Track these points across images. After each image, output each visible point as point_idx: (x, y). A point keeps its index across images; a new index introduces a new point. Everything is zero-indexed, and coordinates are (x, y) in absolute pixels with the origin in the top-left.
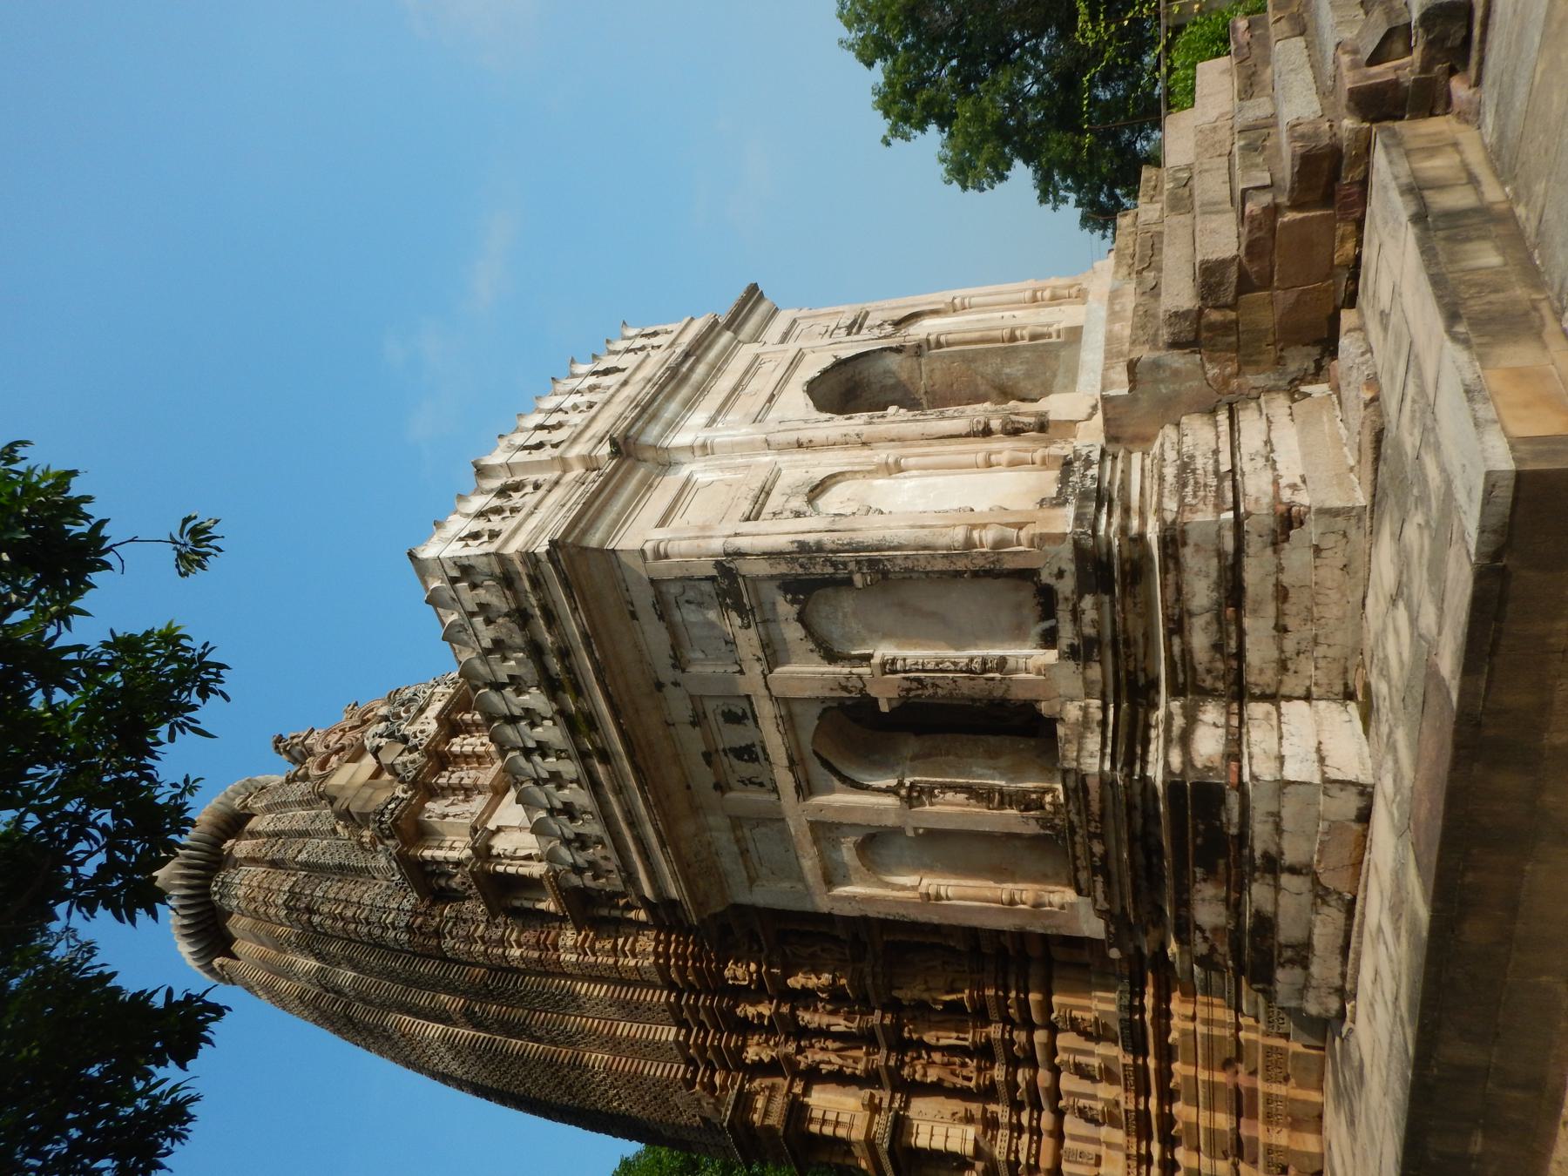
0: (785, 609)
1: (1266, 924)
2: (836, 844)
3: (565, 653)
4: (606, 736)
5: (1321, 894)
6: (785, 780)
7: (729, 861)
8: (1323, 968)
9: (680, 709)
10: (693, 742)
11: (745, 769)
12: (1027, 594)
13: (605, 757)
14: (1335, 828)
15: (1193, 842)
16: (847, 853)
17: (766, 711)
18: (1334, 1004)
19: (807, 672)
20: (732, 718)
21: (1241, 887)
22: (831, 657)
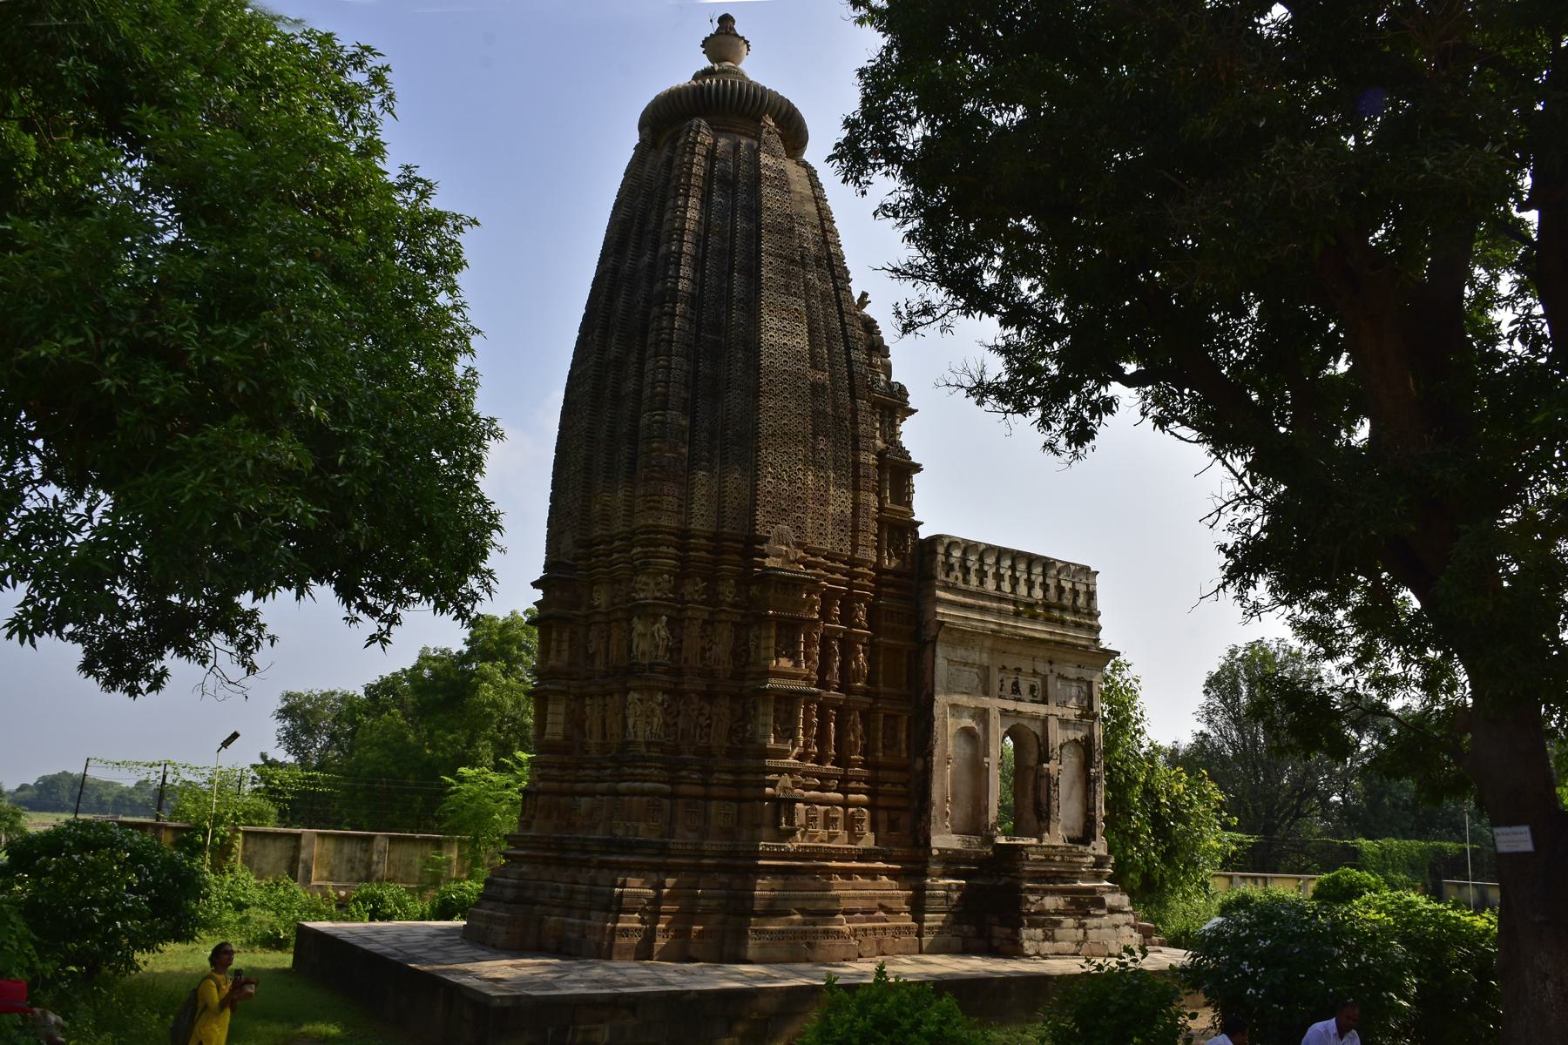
0: (1080, 735)
1: (1058, 924)
2: (973, 717)
3: (1063, 623)
4: (1024, 621)
5: (1079, 943)
6: (1010, 705)
7: (960, 653)
8: (1047, 947)
9: (1042, 668)
10: (1026, 666)
11: (1008, 684)
12: (1078, 833)
13: (1017, 614)
14: (1106, 947)
15: (1082, 897)
16: (967, 722)
17: (1042, 710)
18: (1030, 952)
19: (1057, 736)
20: (1032, 689)
21: (1065, 913)
22: (1061, 747)
